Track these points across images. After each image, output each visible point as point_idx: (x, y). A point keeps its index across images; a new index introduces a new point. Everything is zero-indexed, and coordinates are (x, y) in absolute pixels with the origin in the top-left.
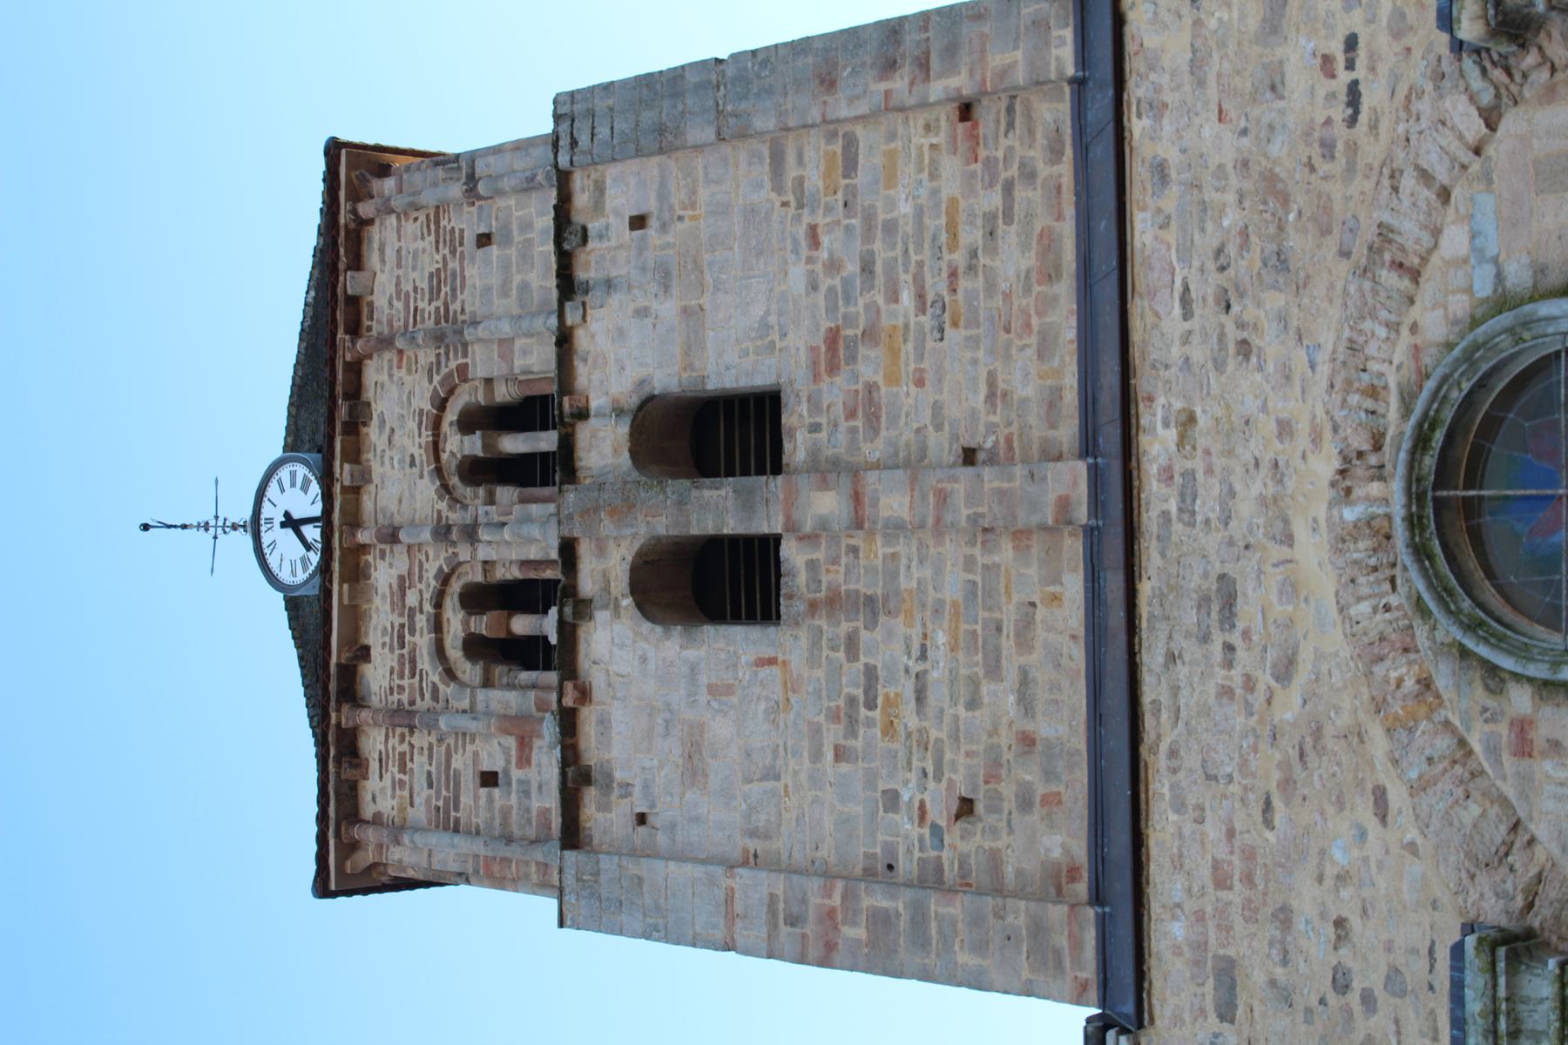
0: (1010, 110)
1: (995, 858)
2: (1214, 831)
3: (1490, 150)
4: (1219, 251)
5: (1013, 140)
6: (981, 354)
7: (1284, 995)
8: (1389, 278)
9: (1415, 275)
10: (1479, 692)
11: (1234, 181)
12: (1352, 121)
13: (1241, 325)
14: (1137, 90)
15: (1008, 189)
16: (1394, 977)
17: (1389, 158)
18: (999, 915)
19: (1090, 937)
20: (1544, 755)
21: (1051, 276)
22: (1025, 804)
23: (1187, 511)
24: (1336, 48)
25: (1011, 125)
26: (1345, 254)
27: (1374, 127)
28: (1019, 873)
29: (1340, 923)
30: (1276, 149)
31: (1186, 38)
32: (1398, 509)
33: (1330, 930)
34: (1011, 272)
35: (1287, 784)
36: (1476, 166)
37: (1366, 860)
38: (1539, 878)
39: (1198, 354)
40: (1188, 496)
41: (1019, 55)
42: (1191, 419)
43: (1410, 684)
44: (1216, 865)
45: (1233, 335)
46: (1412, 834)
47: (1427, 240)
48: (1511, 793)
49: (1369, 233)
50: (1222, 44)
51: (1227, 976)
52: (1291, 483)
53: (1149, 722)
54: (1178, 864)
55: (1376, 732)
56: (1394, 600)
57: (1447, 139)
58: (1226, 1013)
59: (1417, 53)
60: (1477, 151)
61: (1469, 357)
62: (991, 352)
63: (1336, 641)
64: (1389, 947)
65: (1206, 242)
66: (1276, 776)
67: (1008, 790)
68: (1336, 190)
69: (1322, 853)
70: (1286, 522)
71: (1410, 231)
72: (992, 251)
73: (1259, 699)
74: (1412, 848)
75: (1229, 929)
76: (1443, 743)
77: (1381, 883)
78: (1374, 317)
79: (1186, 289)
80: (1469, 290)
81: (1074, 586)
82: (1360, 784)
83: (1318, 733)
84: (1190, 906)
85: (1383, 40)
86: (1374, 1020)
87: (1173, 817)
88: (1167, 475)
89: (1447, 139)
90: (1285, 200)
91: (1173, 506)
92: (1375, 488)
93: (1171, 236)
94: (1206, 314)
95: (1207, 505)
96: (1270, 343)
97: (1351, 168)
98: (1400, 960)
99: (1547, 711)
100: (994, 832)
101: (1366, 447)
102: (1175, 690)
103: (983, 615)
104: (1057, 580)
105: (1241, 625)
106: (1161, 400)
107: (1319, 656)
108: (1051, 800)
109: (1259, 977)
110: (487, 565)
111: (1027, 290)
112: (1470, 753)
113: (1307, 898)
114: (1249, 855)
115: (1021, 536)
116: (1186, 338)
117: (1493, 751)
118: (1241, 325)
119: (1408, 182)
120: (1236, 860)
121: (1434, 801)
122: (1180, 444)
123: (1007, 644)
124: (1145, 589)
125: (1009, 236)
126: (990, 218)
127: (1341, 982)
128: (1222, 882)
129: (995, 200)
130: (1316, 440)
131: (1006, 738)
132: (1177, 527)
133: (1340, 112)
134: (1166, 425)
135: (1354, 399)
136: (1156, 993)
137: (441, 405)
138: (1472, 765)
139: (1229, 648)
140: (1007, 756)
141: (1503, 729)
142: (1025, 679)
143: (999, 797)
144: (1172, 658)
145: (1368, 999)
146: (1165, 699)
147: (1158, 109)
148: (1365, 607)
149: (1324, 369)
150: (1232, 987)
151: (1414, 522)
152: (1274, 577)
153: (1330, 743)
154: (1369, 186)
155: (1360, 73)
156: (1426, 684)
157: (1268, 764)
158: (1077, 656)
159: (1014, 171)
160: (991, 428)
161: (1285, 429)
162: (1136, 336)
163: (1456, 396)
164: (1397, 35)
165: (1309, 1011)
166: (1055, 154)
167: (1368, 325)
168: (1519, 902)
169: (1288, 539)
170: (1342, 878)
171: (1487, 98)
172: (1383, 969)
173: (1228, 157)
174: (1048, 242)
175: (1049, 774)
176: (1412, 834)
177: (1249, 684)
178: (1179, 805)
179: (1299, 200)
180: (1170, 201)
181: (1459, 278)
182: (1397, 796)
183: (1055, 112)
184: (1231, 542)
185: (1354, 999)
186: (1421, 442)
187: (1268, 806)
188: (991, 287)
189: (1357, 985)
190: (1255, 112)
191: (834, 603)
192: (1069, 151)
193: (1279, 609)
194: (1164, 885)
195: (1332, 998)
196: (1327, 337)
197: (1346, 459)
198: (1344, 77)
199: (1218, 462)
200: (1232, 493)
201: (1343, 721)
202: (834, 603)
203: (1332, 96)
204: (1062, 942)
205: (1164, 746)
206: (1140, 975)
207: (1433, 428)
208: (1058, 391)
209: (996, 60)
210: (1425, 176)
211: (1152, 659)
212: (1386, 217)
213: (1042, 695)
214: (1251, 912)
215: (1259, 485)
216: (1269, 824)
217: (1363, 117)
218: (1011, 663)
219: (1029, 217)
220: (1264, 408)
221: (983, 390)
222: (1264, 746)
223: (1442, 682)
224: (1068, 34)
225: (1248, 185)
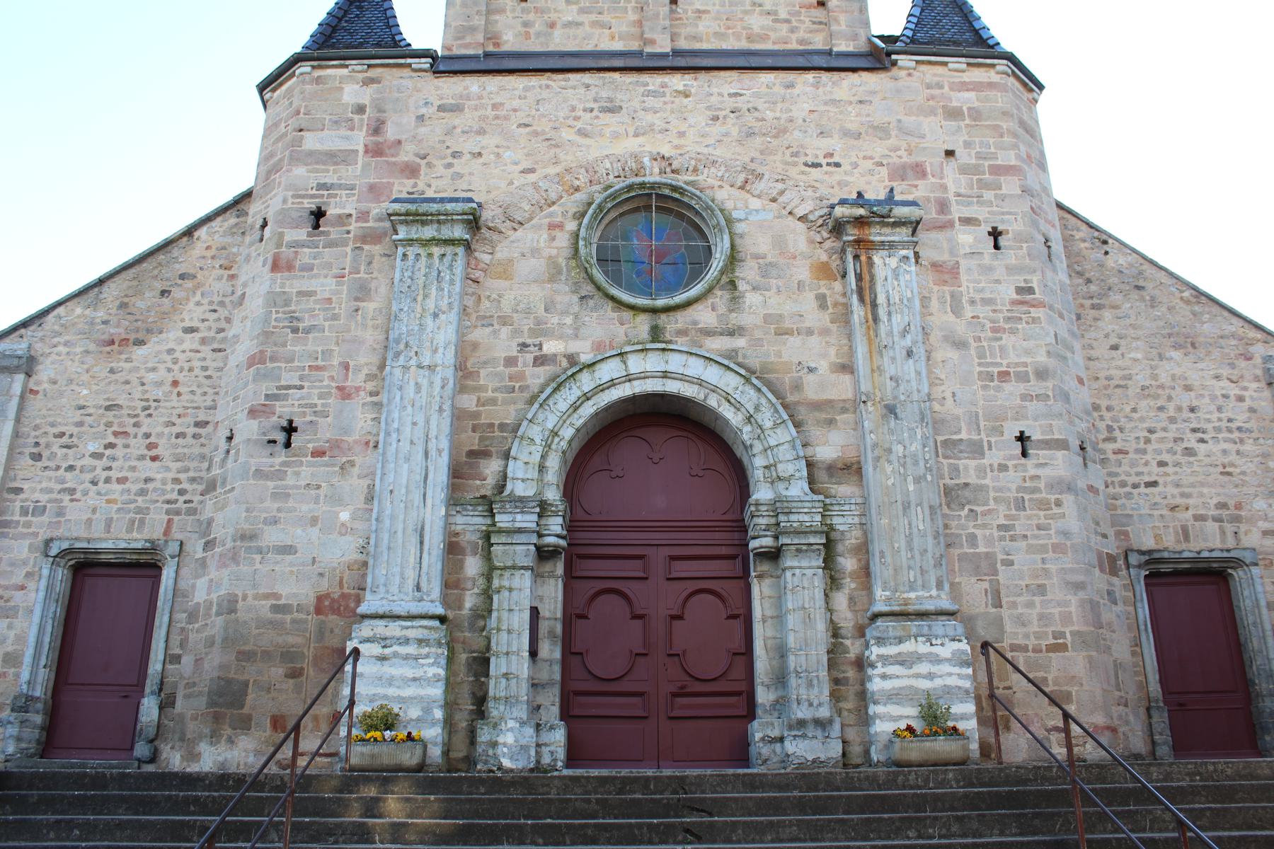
0: (821, 23)
1: (501, 11)
2: (516, 103)
3: (790, 218)
4: (756, 109)
5: (808, 24)
6: (717, 7)
7: (449, 132)
8: (741, 178)
9: (742, 188)
10: (575, 210)
11: (784, 116)
12: (806, 164)
13: (725, 117)
14: (825, 76)
15: (787, 21)
16: (459, 176)
17: (790, 179)
18: (478, 12)
19: (471, 52)
20: (550, 234)
21: (749, 38)
22: (526, 24)
23: (649, 94)
24: (836, 159)
25: (814, 23)
26: (752, 161)
27: (803, 173)
28: (496, 22)
29: (480, 154)
30: (796, 133)
31: (845, 98)
32: (647, 179)
33: (477, 150)
34: (752, 21)
35: (536, 134)
36: (785, 212)
37: (506, 165)
38: (501, 232)
39: (714, 99)
40: (654, 94)
41: (844, 27)
42: (687, 96)
43: (577, 183)
44: (502, 104)
45: (721, 114)
46: (516, 183)
47: (756, 193)
48: (533, 222)
49: (759, 170)
50: (841, 112)
51: (456, 109)
52: (659, 136)
53: (561, 76)
54: (502, 88)
55: (558, 169)
56: (611, 177)
57: (796, 201)
58: (441, 108)
59: (831, 191)
60: (790, 213)
61: (708, 208)
62: (718, 12)
63: (594, 154)
64: (470, 174)
65: (760, 104)
66: (539, 129)
67: (531, 17)
68: (778, 157)
69: (508, 147)
70: (643, 134)
71: (760, 186)
72: (761, 14)
73: (570, 122)
74: (511, 183)
75: (476, 109)
76: (553, 196)
77: (496, 171)
78: (726, 171)
79: (741, 95)
80: (735, 209)
81: (618, 46)
82: (537, 163)
83: (557, 146)
84: (485, 93)
85: (837, 178)
86: (441, 168)
87: (521, 86)
88: (664, 86)
89: (796, 201)
90: (775, 137)
91: (651, 88)
92: (656, 170)
93: (764, 90)
94: (730, 103)
95: (651, 102)
96: (717, 129)
97: (787, 163)
98: (466, 178)
99: (567, 236)
100: (513, 10)
101: (673, 167)
102: (574, 88)
103: (606, 6)
104: (621, 38)
105: (601, 115)
106: (695, 84)
107: (589, 147)
108: (527, 36)
109: (457, 122)
111: (744, 28)
112: (550, 206)
113: (489, 141)
114: (506, 118)
115: (640, 23)
116: (720, 95)
117: (551, 215)
118: (725, 117)
119: (780, 186)
120: (504, 112)
121: (530, 192)
122: (676, 91)
123: (593, 17)
124: (616, 75)
125: (767, 21)
126: (776, 13)
127: (455, 155)
128: (495, 107)
129: (783, 15)
130: (677, 147)
131: (554, 16)
132: (642, 89)
133: (810, 160)
134: (685, 85)
135: (693, 162)
136: (448, 79)
138: (545, 207)
139: (592, 110)
140: (546, 17)
141: (559, 219)
142: (578, 24)
143: (529, 12)
144: (587, 86)
145: (450, 165)
146: (570, 83)
147: (816, 86)
148: (608, 166)
149: (705, 151)
150: (452, 111)
151: (642, 185)
152: (621, 130)
153: (553, 151)
154: (779, 170)
155: (825, 168)
156: (577, 189)
157: (543, 126)
158: (589, 47)
159: (795, 24)
160: (686, 11)
161: (682, 134)
162: (722, 73)
163: (693, 203)
164: (839, 183)
165: (444, 142)
166: (801, 42)
167: (723, 168)
168: (491, 225)
169: (636, 135)
170: (498, 155)
171: (811, 217)
172: (462, 172)
173: (794, 114)
174: (764, 38)
175: (538, 35)
176: (516, 183)
177: (577, 118)
178: (526, 89)
179: (775, 142)
180: (778, 89)
181: (740, 205)
182: (531, 178)
183: (818, 42)
184: (635, 111)
185: (450, 160)
186: (675, 188)
187: (527, 126)
188: (746, 12)
189: (455, 161)
190: (812, 125)
192: (801, 48)
193: (607, 132)
194: (493, 82)
195: (449, 151)
196: (719, 152)
197: (668, 159)
198: (824, 162)
199: (669, 107)
200: (655, 112)
201: (562, 156)
203: (817, 157)
204: (468, 40)
205: (550, 83)
206: (455, 73)
207: (680, 193)
208: (701, 40)
209: (843, 18)
210: (782, 193)
211: (587, 78)
212: (766, 177)
213: (571, 32)
214: (483, 118)
215: (659, 124)
216: (520, 126)
217: (807, 169)
218: (583, 18)
219: (775, 30)
220: (690, 126)
221: (702, 8)
222: (551, 124)
223: (578, 196)
224: (851, 49)
225: (782, 122)
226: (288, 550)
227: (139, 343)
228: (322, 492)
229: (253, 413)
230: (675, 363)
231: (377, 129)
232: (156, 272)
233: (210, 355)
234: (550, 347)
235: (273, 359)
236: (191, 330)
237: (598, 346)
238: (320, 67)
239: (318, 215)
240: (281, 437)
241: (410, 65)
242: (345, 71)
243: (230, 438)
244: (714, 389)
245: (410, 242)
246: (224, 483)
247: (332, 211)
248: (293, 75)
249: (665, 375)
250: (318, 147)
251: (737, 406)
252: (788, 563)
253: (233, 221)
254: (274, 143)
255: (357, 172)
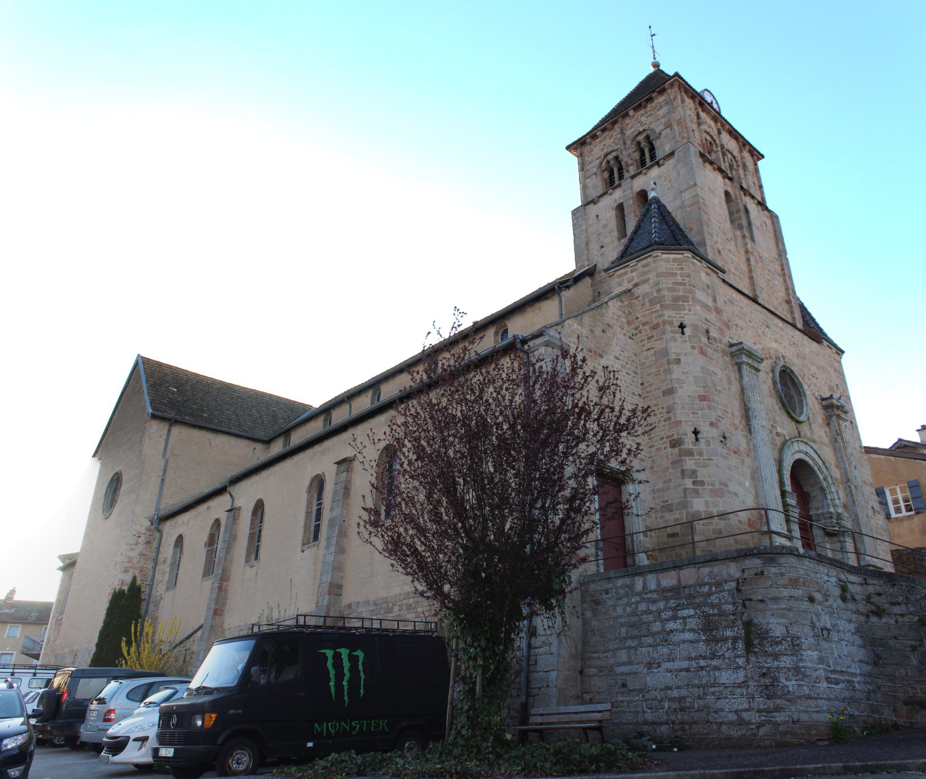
55: (761, 347)
110: (716, 152)
127: (737, 325)
128: (742, 308)
137: (734, 157)
169: (776, 342)
191: (736, 239)
202: (736, 239)
226: (736, 495)
227: (601, 356)
228: (740, 470)
229: (712, 424)
230: (808, 450)
231: (715, 301)
232: (599, 317)
233: (626, 375)
234: (779, 430)
235: (713, 401)
236: (617, 358)
237: (789, 434)
238: (693, 257)
239: (707, 332)
240: (723, 440)
241: (717, 273)
242: (699, 264)
243: (696, 432)
244: (816, 464)
245: (748, 364)
246: (701, 454)
247: (711, 334)
248: (682, 254)
249: (806, 454)
250: (700, 299)
251: (822, 473)
252: (846, 539)
253: (619, 303)
254: (673, 283)
255: (713, 316)
